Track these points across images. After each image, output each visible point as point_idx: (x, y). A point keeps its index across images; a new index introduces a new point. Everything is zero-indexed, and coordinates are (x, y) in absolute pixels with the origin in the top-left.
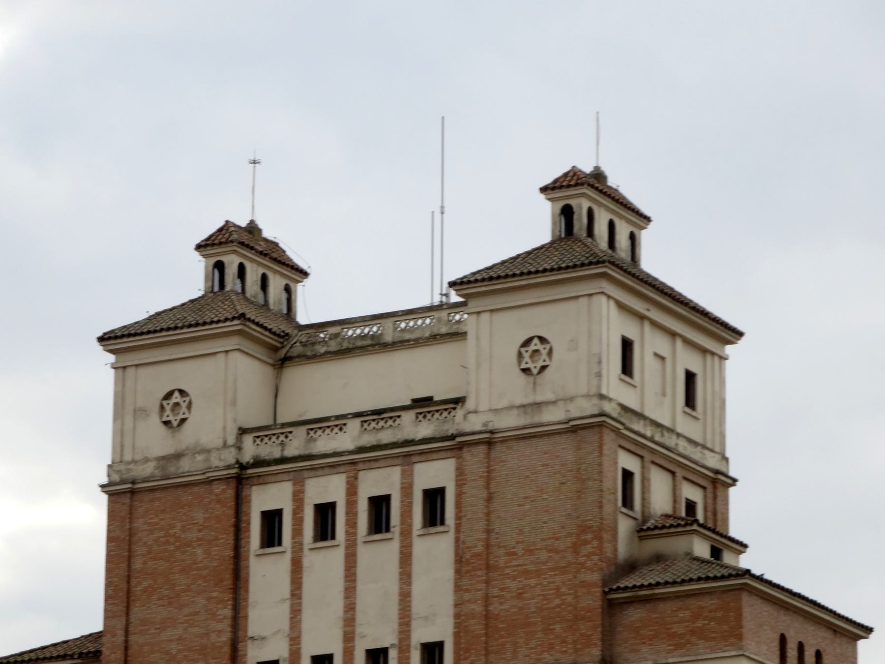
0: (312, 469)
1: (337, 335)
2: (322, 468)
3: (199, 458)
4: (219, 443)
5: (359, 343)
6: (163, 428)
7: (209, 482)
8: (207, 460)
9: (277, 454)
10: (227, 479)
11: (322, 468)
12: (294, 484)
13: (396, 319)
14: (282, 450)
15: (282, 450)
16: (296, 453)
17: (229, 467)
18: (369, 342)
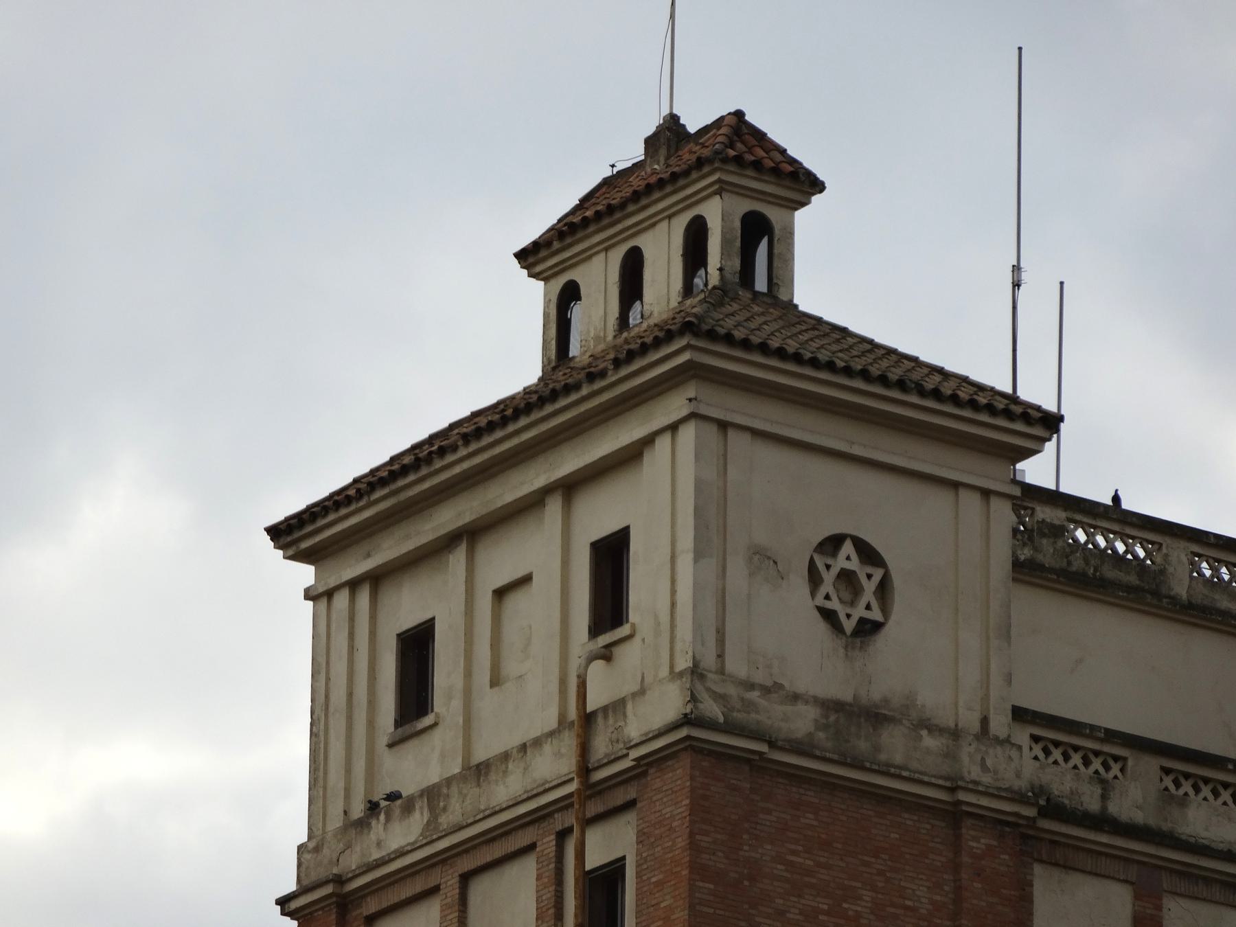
0: (1185, 874)
1: (1058, 531)
2: (1208, 881)
3: (930, 742)
4: (970, 720)
5: (1110, 573)
6: (821, 626)
7: (954, 815)
8: (950, 755)
9: (1091, 801)
10: (998, 824)
11: (1208, 881)
12: (1137, 897)
13: (1196, 548)
14: (1104, 797)
15: (1104, 797)
16: (1139, 817)
17: (1018, 797)
18: (1133, 579)
